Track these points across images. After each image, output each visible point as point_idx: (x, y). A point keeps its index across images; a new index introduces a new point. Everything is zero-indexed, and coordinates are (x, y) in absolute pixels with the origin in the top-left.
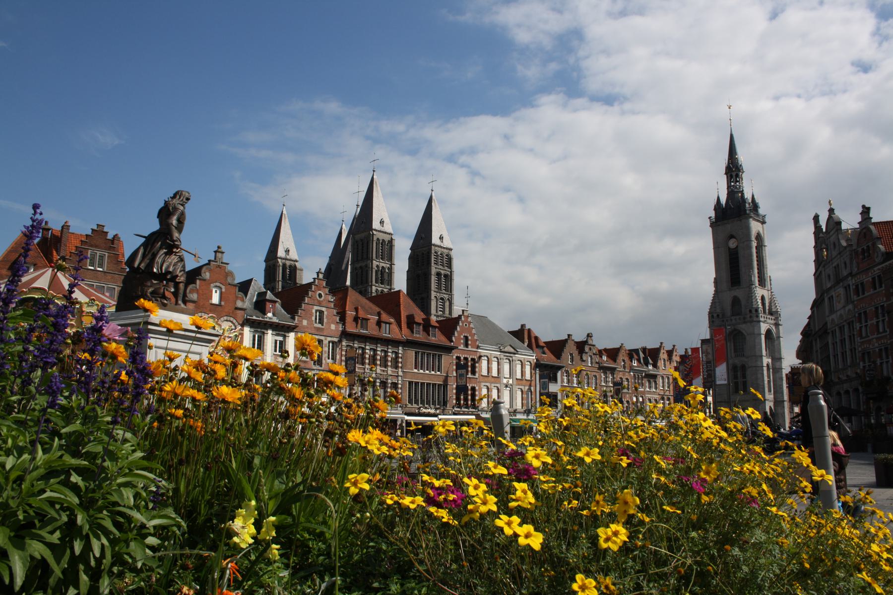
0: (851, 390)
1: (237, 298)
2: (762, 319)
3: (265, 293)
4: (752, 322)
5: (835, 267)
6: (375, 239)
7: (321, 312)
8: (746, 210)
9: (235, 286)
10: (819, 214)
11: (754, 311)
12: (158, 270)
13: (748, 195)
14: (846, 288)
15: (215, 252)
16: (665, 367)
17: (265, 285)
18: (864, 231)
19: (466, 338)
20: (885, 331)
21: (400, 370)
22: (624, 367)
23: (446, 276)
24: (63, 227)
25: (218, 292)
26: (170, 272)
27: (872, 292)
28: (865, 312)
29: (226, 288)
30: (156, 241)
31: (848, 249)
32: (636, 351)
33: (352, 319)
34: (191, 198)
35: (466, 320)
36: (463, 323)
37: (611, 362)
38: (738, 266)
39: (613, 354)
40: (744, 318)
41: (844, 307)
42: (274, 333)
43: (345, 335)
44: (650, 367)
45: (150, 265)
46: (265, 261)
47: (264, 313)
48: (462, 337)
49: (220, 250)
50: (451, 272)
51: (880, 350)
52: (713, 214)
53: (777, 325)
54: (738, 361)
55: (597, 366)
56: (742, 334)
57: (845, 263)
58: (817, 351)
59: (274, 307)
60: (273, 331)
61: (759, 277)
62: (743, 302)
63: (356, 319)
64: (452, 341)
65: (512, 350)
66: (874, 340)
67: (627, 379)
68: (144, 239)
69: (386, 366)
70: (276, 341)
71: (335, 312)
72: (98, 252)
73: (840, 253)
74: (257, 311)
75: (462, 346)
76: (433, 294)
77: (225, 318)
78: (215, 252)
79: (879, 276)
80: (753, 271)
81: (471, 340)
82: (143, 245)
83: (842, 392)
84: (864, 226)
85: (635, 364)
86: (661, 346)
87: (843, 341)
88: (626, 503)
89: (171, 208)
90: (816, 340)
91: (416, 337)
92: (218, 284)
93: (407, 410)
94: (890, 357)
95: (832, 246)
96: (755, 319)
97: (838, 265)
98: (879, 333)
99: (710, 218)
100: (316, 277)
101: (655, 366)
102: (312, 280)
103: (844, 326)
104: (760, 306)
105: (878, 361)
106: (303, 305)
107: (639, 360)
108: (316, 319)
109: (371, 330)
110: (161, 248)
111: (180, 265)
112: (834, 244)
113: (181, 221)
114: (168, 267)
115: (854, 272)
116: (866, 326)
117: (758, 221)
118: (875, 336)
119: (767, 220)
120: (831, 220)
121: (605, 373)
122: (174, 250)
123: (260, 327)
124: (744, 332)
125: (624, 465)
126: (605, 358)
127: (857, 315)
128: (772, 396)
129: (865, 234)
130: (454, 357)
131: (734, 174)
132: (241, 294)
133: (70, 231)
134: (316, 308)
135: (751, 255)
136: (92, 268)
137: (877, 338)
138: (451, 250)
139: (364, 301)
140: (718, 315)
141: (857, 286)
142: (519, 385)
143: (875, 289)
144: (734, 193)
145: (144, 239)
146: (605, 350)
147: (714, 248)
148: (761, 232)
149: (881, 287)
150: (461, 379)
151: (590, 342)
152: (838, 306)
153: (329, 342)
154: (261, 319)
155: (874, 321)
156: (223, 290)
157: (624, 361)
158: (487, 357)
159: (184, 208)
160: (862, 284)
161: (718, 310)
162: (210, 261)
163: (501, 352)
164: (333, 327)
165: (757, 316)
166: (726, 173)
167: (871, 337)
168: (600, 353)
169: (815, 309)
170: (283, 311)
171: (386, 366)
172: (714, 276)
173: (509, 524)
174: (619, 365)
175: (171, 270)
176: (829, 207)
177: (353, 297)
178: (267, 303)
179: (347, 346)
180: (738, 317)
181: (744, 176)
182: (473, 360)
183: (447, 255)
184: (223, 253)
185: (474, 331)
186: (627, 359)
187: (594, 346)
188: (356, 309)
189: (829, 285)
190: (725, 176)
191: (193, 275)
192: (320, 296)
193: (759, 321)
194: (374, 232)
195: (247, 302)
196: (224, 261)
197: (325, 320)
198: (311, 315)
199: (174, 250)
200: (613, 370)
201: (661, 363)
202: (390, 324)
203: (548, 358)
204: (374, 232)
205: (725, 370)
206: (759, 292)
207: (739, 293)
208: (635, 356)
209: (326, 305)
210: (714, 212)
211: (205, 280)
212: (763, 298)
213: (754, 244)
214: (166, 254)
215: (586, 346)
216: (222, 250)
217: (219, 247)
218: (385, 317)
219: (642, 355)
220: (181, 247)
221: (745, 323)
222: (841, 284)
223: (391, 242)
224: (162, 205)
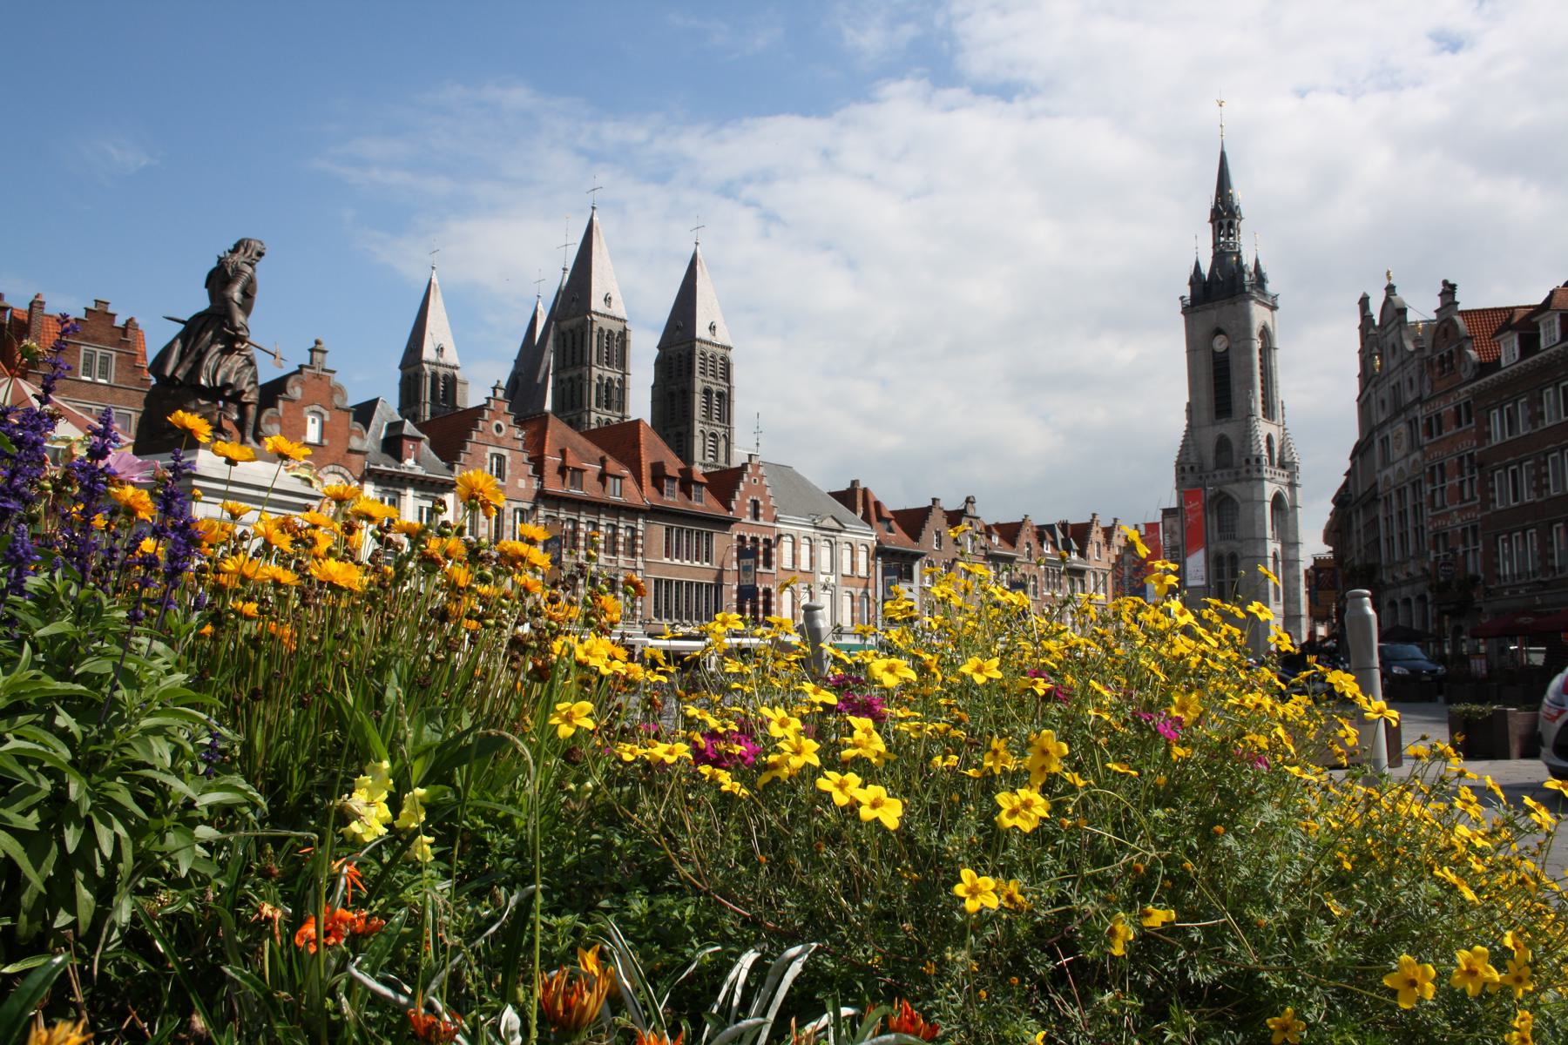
0: (1413, 598)
1: (351, 432)
2: (1267, 476)
3: (401, 424)
4: (1251, 479)
6: (595, 328)
7: (501, 458)
8: (1244, 286)
9: (347, 410)
10: (1369, 294)
11: (1253, 462)
12: (208, 380)
13: (1248, 261)
14: (1410, 423)
15: (312, 350)
16: (1099, 555)
17: (401, 410)
19: (756, 504)
20: (1473, 498)
21: (640, 559)
22: (1030, 556)
23: (720, 395)
24: (31, 304)
25: (317, 421)
26: (230, 386)
27: (1454, 430)
28: (1441, 466)
29: (331, 416)
30: (203, 329)
31: (1416, 356)
32: (1051, 528)
33: (556, 470)
34: (266, 252)
35: (755, 473)
36: (749, 476)
37: (1007, 546)
38: (1228, 383)
39: (1010, 532)
40: (1237, 473)
41: (1407, 456)
42: (418, 494)
43: (543, 497)
44: (1074, 556)
45: (194, 372)
46: (401, 367)
47: (399, 458)
48: (748, 501)
49: (319, 347)
50: (729, 388)
51: (1464, 530)
52: (1187, 292)
53: (1292, 486)
54: (1224, 548)
55: (982, 553)
56: (1233, 501)
57: (1411, 381)
58: (1358, 532)
59: (417, 449)
60: (415, 490)
61: (1263, 402)
62: (1236, 446)
63: (562, 470)
64: (730, 509)
65: (835, 525)
66: (1455, 513)
67: (1035, 577)
68: (182, 326)
69: (615, 552)
70: (421, 509)
71: (525, 457)
72: (99, 352)
73: (1403, 363)
74: (387, 456)
75: (748, 517)
76: (698, 427)
77: (331, 468)
78: (312, 350)
79: (1467, 404)
80: (1253, 392)
81: (764, 508)
82: (179, 336)
83: (1398, 601)
84: (1444, 317)
85: (1048, 549)
86: (1092, 521)
87: (1402, 515)
88: (1045, 753)
89: (229, 270)
90: (1358, 512)
91: (668, 502)
92: (317, 408)
93: (652, 629)
94: (1480, 542)
95: (1390, 351)
96: (1255, 474)
97: (1398, 384)
98: (1463, 500)
99: (1182, 298)
100: (491, 395)
101: (1082, 553)
102: (485, 402)
103: (1405, 488)
104: (1265, 452)
105: (1461, 550)
106: (469, 445)
107: (1054, 544)
108: (491, 469)
109: (589, 489)
110: (213, 342)
111: (248, 372)
112: (1394, 346)
113: (248, 294)
114: (227, 375)
115: (1425, 397)
116: (1442, 489)
117: (1264, 304)
118: (1457, 506)
119: (1279, 303)
120: (1389, 305)
121: (996, 566)
122: (238, 346)
123: (393, 483)
124: (1235, 497)
125: (1041, 692)
126: (996, 540)
127: (1427, 470)
128: (1281, 608)
129: (1446, 330)
130: (735, 537)
131: (1225, 222)
132: (358, 426)
133: (46, 311)
134: (491, 450)
135: (1250, 365)
136: (88, 379)
137: (1458, 510)
138: (729, 348)
139: (576, 438)
140: (1192, 468)
141: (1429, 420)
142: (847, 586)
143: (1460, 425)
144: (1225, 255)
145: (182, 326)
146: (997, 526)
147: (1188, 351)
148: (1270, 324)
149: (1469, 421)
150: (745, 575)
151: (971, 512)
152: (1396, 454)
153: (515, 510)
154: (394, 469)
155: (1456, 481)
156: (327, 418)
157: (1028, 545)
158: (792, 536)
159: (254, 270)
160: (1438, 416)
161: (1193, 459)
162: (301, 367)
163: (816, 528)
164: (522, 483)
165: (1259, 471)
166: (1212, 221)
167: (1449, 508)
168: (988, 531)
169: (1358, 458)
170: (433, 455)
171: (615, 552)
172: (1186, 399)
173: (842, 786)
174: (1020, 553)
175: (232, 380)
176: (1386, 283)
177: (557, 430)
178: (405, 442)
179: (547, 517)
180: (1225, 471)
181: (1243, 225)
182: (767, 541)
183: (722, 359)
184: (324, 352)
185: (769, 492)
186: (1034, 542)
187: (977, 518)
188: (563, 453)
189: (1382, 418)
190: (1210, 225)
191: (272, 392)
192: (499, 428)
193: (1263, 479)
194: (594, 317)
195: (370, 440)
196: (327, 367)
197: (508, 472)
198: (483, 462)
199: (238, 346)
200: (1010, 560)
201: (1092, 550)
202: (621, 478)
203: (898, 539)
204: (594, 317)
205: (1203, 562)
206: (1263, 428)
207: (1228, 429)
208: (1049, 537)
209: (507, 445)
210: (1189, 288)
211: (293, 401)
212: (1269, 439)
213: (1257, 345)
214: (223, 352)
215: (964, 519)
216: (323, 346)
217: (317, 342)
218: (613, 466)
219: (1060, 536)
220: (250, 340)
221: (1237, 481)
222: (1403, 416)
223: (623, 334)
224: (214, 264)
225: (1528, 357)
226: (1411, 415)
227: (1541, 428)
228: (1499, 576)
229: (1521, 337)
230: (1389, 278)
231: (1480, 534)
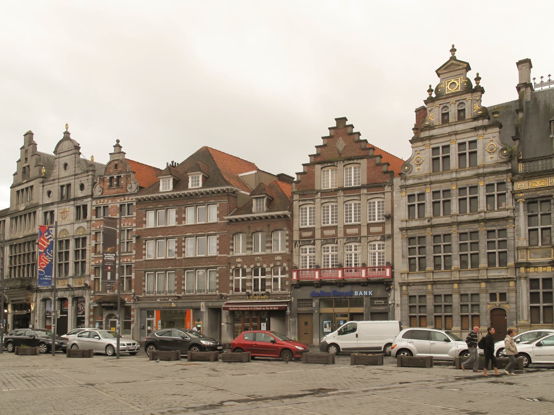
5: (62, 187)
14: (78, 208)
18: (116, 162)
73: (75, 175)
95: (62, 167)
97: (69, 185)
127: (93, 233)
141: (97, 208)
176: (65, 130)
189: (47, 201)
222: (72, 203)
225: (177, 191)
226: (79, 203)
227: (183, 224)
228: (145, 292)
229: (174, 179)
230: (67, 128)
231: (133, 270)
